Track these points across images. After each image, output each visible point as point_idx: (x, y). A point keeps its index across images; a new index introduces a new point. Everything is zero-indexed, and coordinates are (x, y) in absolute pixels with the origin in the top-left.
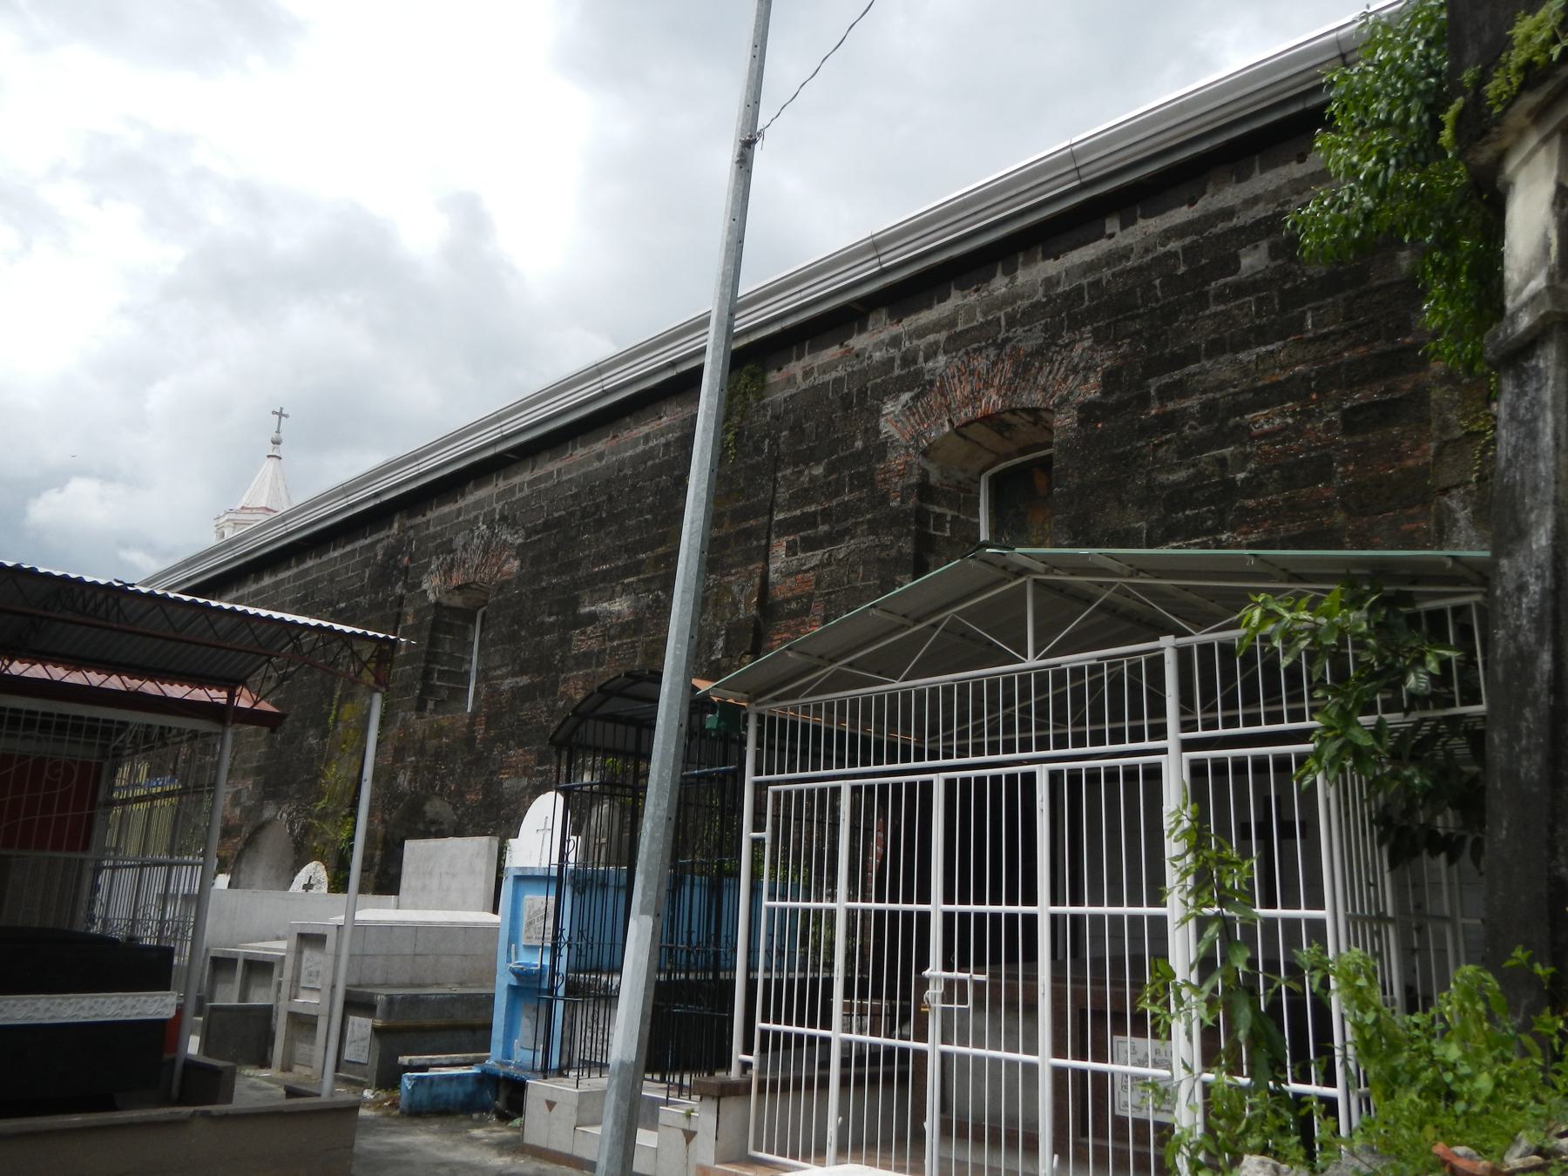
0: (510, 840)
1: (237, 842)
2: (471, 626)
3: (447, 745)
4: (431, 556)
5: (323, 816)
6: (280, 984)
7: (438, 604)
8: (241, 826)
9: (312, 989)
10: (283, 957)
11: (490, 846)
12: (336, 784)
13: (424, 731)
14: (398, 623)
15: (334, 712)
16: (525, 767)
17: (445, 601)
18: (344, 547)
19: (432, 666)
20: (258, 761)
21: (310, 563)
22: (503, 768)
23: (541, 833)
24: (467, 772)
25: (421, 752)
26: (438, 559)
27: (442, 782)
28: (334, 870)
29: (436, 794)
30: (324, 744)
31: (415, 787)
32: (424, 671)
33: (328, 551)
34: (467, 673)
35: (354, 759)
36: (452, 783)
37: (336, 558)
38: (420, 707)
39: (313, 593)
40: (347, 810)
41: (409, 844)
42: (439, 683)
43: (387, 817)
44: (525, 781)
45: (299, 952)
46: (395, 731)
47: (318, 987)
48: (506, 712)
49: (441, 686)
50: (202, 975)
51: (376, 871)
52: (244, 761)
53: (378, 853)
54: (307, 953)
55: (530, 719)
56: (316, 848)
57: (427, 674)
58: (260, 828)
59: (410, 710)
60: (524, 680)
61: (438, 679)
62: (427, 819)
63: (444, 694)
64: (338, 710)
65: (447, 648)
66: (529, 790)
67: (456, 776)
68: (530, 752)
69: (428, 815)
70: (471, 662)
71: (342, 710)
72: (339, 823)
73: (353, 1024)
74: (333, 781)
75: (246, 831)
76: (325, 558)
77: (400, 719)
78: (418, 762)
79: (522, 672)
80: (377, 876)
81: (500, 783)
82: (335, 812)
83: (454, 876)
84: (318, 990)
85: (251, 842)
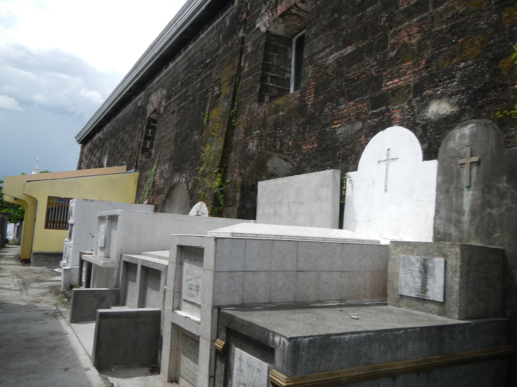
0: (348, 173)
1: (162, 196)
2: (289, 48)
3: (283, 116)
4: (261, 5)
5: (204, 175)
6: (165, 292)
7: (268, 32)
8: (163, 189)
9: (193, 303)
10: (167, 267)
11: (334, 177)
12: (210, 155)
13: (265, 112)
14: (241, 54)
15: (206, 116)
16: (358, 114)
17: (272, 30)
18: (207, 30)
19: (266, 73)
20: (171, 154)
21: (190, 47)
22: (335, 120)
23: (383, 165)
24: (301, 130)
25: (264, 125)
26: (266, 4)
27: (281, 141)
28: (212, 206)
29: (276, 151)
30: (202, 137)
31: (261, 149)
32: (261, 76)
33: (199, 36)
34: (288, 79)
35: (220, 139)
36: (290, 140)
37: (204, 37)
38: (261, 100)
39: (193, 61)
40: (218, 169)
41: (261, 185)
42: (271, 84)
43: (242, 171)
44: (359, 125)
45: (180, 265)
46: (245, 117)
47: (200, 303)
48: (333, 79)
49: (273, 86)
50: (119, 274)
51: (238, 206)
52: (164, 156)
53: (238, 194)
54: (187, 266)
55: (358, 77)
56: (200, 194)
57: (263, 78)
58: (173, 188)
59: (254, 102)
60: (349, 50)
61: (271, 82)
62: (268, 173)
63: (275, 92)
64: (208, 114)
65: (275, 61)
66: (364, 131)
67: (293, 135)
68: (362, 101)
69: (269, 169)
70: (290, 72)
72: (213, 178)
73: (240, 359)
75: (166, 190)
76: (198, 40)
77: (247, 110)
78: (262, 132)
79: (345, 45)
80: (239, 209)
81: (334, 131)
82: (211, 172)
83: (301, 203)
84: (199, 306)
85: (169, 196)
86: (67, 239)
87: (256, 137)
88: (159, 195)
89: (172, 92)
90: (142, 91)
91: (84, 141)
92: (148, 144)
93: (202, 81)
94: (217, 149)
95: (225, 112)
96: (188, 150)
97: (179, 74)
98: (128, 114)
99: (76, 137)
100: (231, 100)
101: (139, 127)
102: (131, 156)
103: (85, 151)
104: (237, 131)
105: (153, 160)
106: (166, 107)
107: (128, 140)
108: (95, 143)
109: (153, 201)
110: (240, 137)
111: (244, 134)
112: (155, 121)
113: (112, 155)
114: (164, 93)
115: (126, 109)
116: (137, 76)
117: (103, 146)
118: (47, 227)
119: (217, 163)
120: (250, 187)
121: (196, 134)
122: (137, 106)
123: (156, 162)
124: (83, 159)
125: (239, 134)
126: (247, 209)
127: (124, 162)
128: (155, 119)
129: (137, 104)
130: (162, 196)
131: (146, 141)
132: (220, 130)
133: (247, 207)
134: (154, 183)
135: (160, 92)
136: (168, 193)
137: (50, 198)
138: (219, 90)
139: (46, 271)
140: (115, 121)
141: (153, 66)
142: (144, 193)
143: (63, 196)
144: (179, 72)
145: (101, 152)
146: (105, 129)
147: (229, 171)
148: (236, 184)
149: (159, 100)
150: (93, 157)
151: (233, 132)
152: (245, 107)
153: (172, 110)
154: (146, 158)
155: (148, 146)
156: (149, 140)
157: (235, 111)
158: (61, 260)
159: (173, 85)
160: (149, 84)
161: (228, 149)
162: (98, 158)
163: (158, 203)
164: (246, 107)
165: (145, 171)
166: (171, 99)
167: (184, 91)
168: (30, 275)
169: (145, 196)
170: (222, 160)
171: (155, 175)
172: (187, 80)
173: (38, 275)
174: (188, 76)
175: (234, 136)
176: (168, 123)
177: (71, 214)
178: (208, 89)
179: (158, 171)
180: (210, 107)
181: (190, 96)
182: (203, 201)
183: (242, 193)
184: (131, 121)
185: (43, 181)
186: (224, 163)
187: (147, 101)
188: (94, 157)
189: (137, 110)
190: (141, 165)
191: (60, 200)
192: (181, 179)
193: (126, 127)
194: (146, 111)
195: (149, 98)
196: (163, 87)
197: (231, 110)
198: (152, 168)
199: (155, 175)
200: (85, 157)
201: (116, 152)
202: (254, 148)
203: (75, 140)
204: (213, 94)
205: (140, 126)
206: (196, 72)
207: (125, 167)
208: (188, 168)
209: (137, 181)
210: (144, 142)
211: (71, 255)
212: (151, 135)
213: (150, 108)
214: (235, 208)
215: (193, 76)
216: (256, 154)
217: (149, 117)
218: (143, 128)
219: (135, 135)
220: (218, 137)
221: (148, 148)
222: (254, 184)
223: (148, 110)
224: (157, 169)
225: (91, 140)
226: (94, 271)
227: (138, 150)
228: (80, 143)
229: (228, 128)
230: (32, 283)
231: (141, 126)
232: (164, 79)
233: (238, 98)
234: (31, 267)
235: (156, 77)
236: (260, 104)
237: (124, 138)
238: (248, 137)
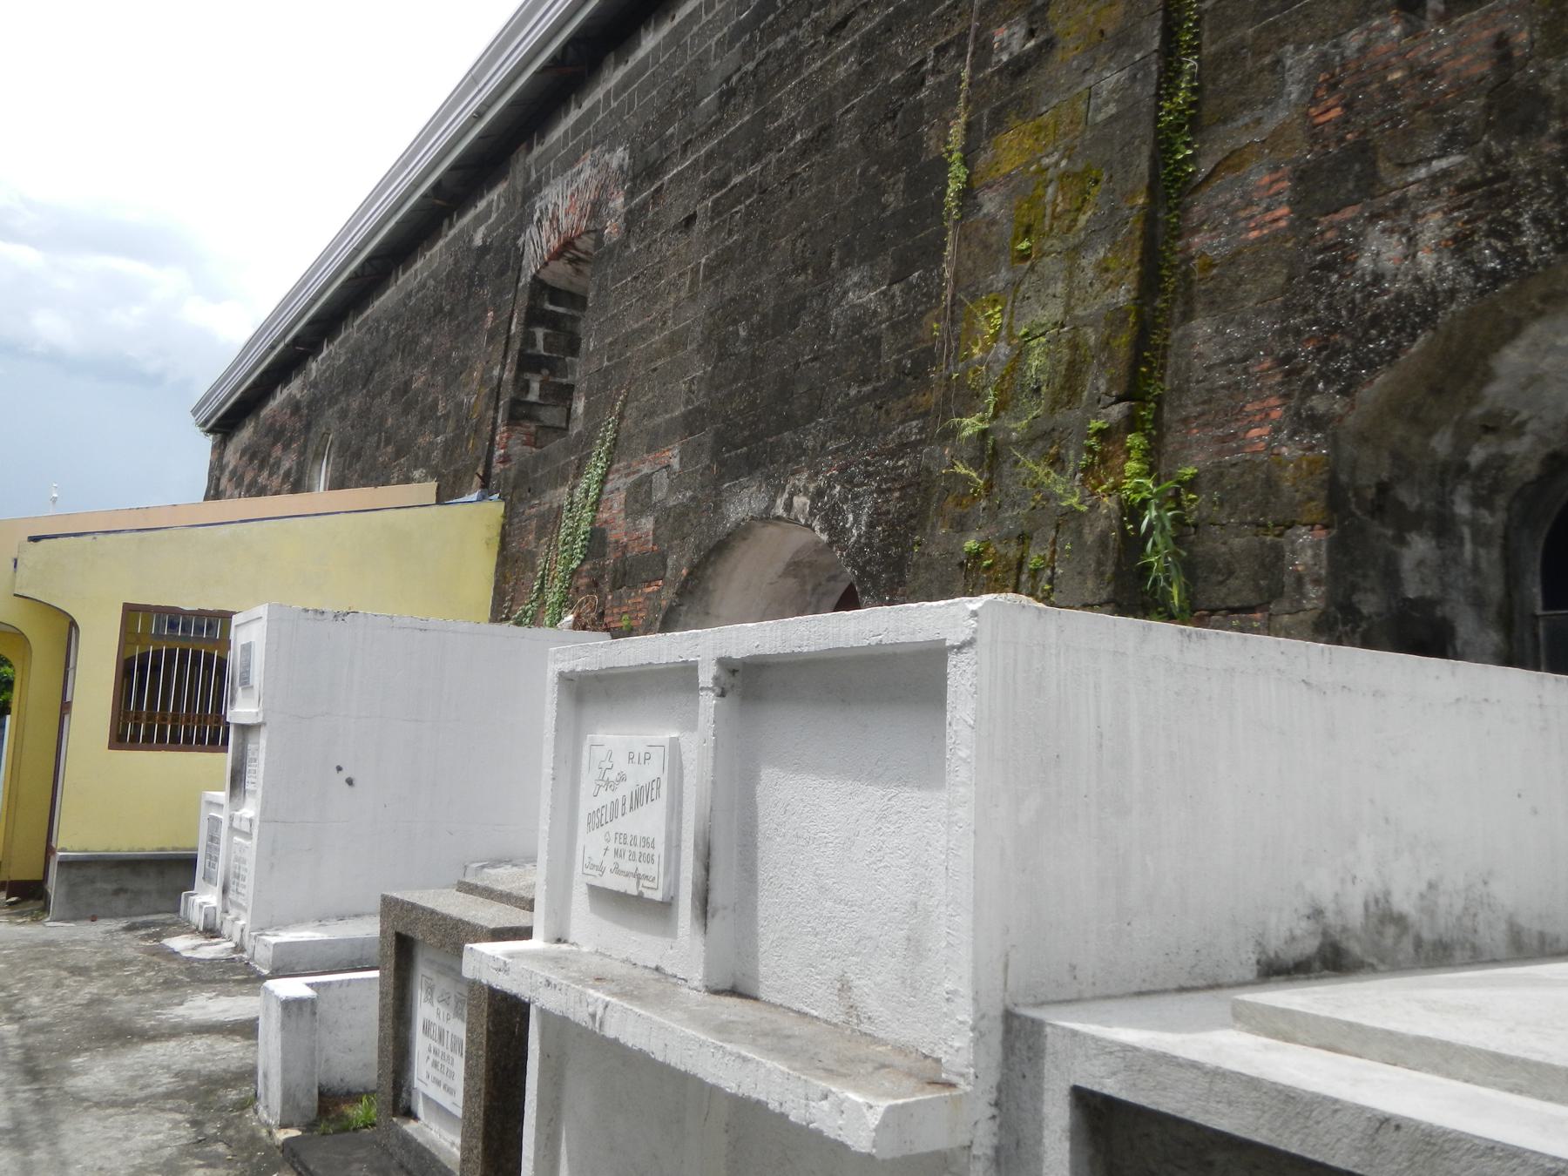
8: (663, 558)
12: (1021, 354)
13: (1501, 42)
20: (688, 402)
40: (1117, 411)
52: (651, 414)
56: (977, 556)
58: (719, 549)
69: (1493, 389)
71: (983, 159)
74: (1003, 349)
75: (678, 564)
77: (1299, 73)
86: (222, 796)
87: (1435, 194)
88: (634, 587)
89: (664, 145)
90: (491, 187)
91: (224, 425)
92: (535, 386)
93: (869, 44)
94: (1079, 312)
95: (1112, 119)
96: (817, 365)
97: (701, 60)
98: (423, 286)
99: (195, 412)
100: (1156, 45)
101: (488, 325)
102: (449, 449)
103: (232, 457)
104: (1221, 199)
105: (586, 441)
106: (632, 218)
107: (428, 384)
108: (272, 425)
109: (602, 615)
110: (1259, 227)
111: (1289, 203)
112: (556, 295)
113: (357, 455)
114: (614, 164)
115: (412, 270)
116: (479, 115)
117: (308, 427)
118: (119, 740)
119: (1098, 382)
120: (1370, 494)
121: (855, 284)
122: (469, 249)
123: (600, 450)
124: (222, 487)
125: (1243, 214)
126: (1364, 625)
127: (417, 474)
128: (561, 284)
129: (471, 240)
130: (650, 589)
131: (528, 376)
132: (1083, 219)
133: (1365, 610)
134: (597, 540)
135: (594, 165)
136: (690, 574)
137: (130, 611)
138: (1031, 34)
139: (129, 952)
140: (359, 328)
141: (555, 62)
142: (542, 583)
143: (188, 605)
144: (707, 51)
145: (302, 452)
146: (314, 367)
147: (1185, 421)
148: (1271, 484)
149: (589, 196)
150: (266, 473)
151: (1186, 210)
152: (1278, 61)
153: (677, 216)
154: (525, 443)
155: (533, 397)
156: (538, 372)
157: (1184, 100)
158: (190, 885)
159: (666, 118)
160: (530, 149)
161: (1159, 304)
162: (287, 474)
163: (634, 623)
164: (1289, 62)
165: (535, 492)
166: (666, 173)
167: (747, 118)
168: (58, 985)
169: (551, 598)
170: (1137, 360)
171: (597, 502)
172: (754, 73)
173: (92, 989)
174: (761, 55)
175: (1196, 230)
176: (659, 276)
177: (245, 682)
178: (923, 62)
179: (618, 482)
180: (969, 126)
181: (791, 128)
182: (1016, 591)
183: (1334, 532)
184: (438, 310)
185: (100, 537)
186: (1150, 375)
187: (521, 212)
188: (270, 475)
189: (466, 267)
190: (512, 474)
191: (173, 626)
192: (780, 502)
193: (415, 340)
194: (520, 257)
195: (533, 205)
196: (609, 140)
197: (1158, 97)
198: (579, 474)
199: (597, 502)
200: (230, 480)
201: (373, 439)
202: (1427, 260)
203: (193, 419)
204: (976, 68)
205: (490, 320)
206: (818, 18)
207: (432, 486)
208: (823, 446)
209: (498, 539)
210: (517, 379)
211: (250, 870)
212: (545, 350)
213: (538, 243)
214: (1286, 618)
215: (794, 40)
216: (1452, 294)
217: (534, 277)
218: (510, 324)
219: (465, 361)
220: (1076, 251)
221: (533, 404)
222: (1385, 476)
223: (530, 250)
224: (611, 477)
225: (258, 416)
226: (545, 1056)
227: (491, 413)
228: (210, 431)
229: (1151, 190)
230: (78, 1053)
231: (495, 318)
232: (614, 104)
233: (1197, 36)
234: (53, 930)
235: (567, 114)
236: (1408, 21)
237: (407, 384)
238: (1349, 212)
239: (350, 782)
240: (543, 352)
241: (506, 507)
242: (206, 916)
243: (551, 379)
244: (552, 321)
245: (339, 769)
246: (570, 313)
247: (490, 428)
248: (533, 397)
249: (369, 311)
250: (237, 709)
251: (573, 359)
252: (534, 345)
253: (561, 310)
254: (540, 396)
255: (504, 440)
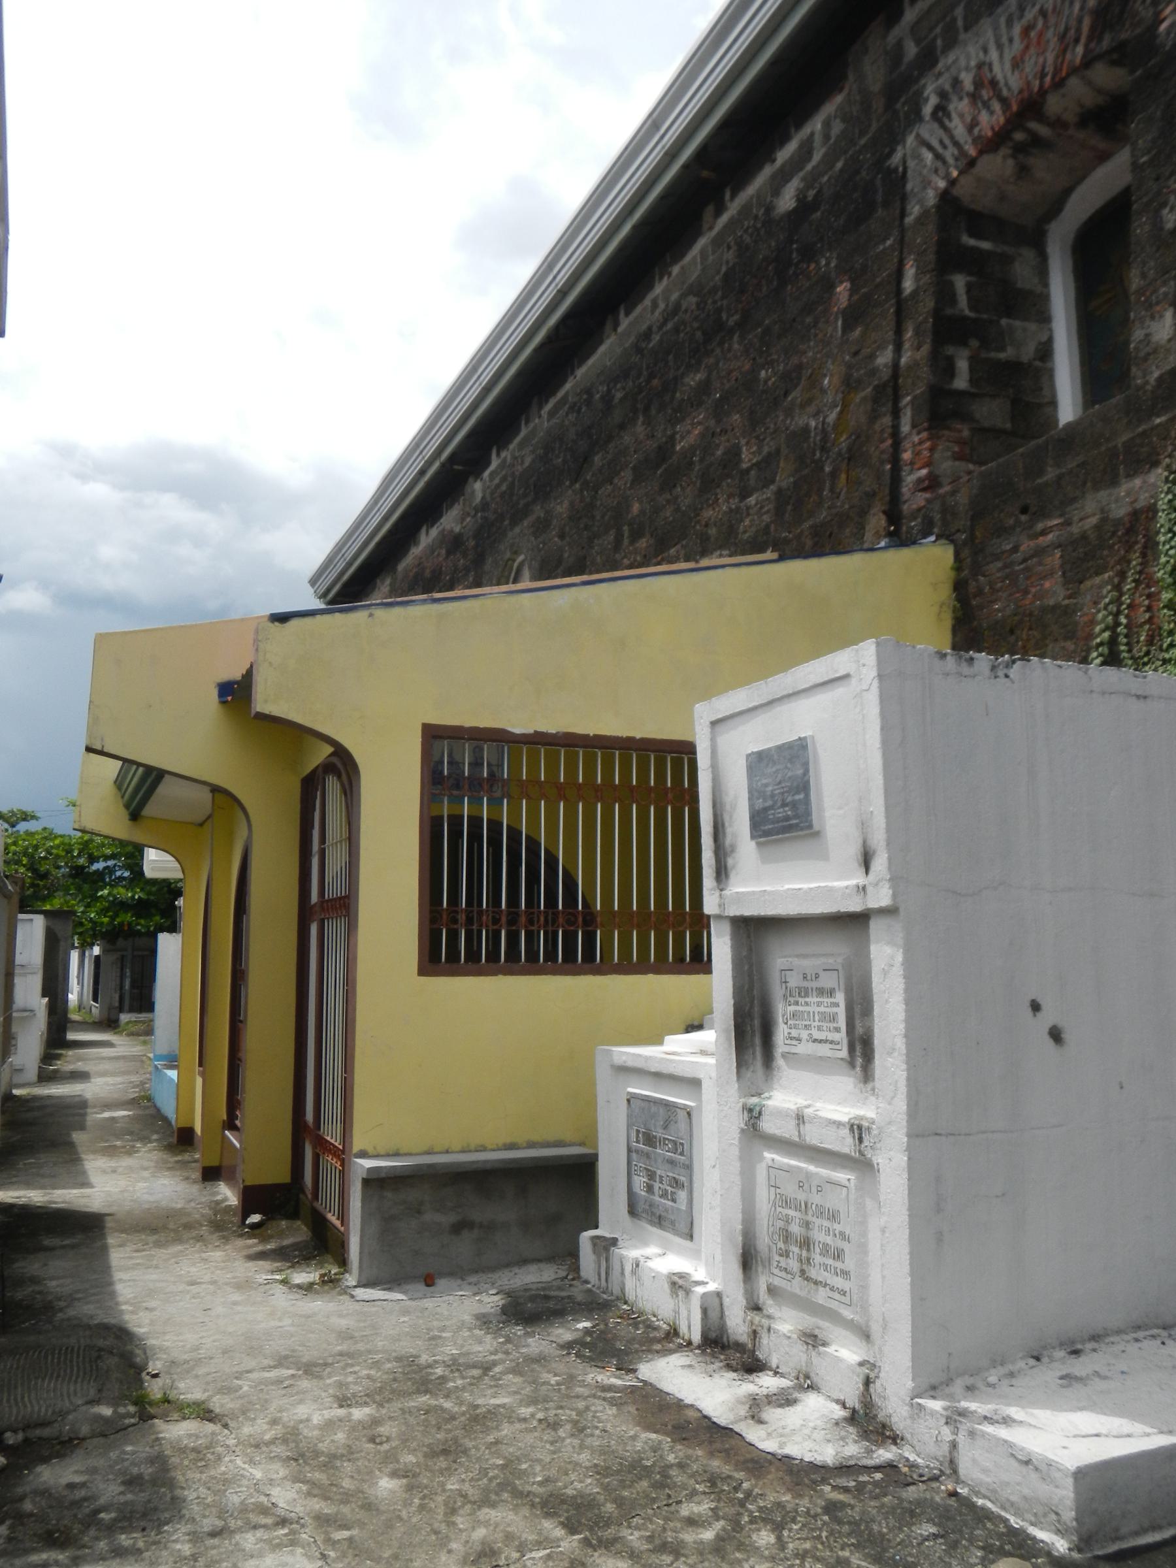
99: (313, 582)
112: (977, 222)
131: (950, 350)
137: (432, 735)
143: (519, 726)
146: (477, 488)
154: (958, 457)
155: (961, 382)
156: (964, 344)
203: (312, 591)
210: (935, 355)
212: (972, 307)
217: (945, 197)
239: (1056, 1035)
240: (967, 312)
241: (957, 555)
242: (705, 1311)
243: (984, 355)
244: (972, 262)
245: (1036, 1007)
246: (999, 250)
247: (889, 442)
248: (961, 382)
249: (568, 386)
250: (738, 886)
251: (1011, 321)
252: (953, 300)
253: (985, 245)
254: (971, 381)
255: (926, 453)
